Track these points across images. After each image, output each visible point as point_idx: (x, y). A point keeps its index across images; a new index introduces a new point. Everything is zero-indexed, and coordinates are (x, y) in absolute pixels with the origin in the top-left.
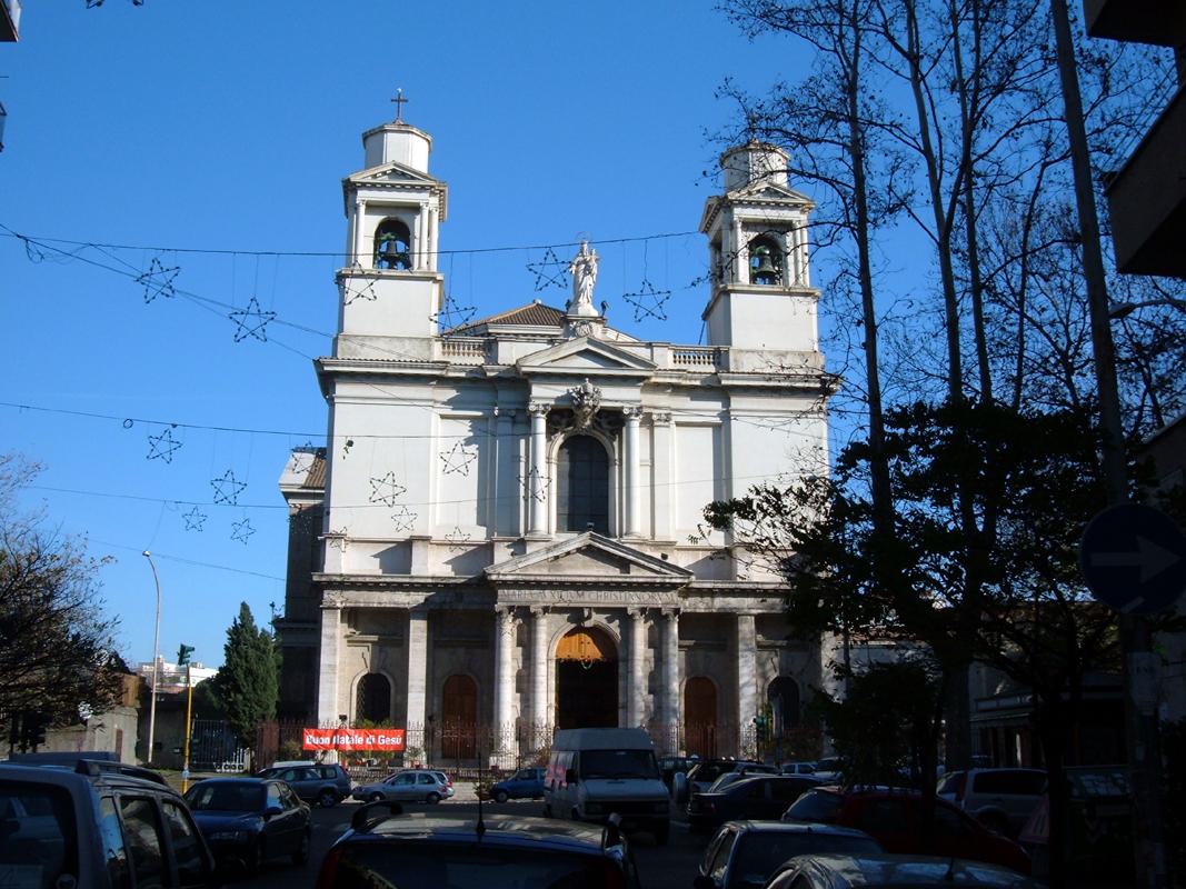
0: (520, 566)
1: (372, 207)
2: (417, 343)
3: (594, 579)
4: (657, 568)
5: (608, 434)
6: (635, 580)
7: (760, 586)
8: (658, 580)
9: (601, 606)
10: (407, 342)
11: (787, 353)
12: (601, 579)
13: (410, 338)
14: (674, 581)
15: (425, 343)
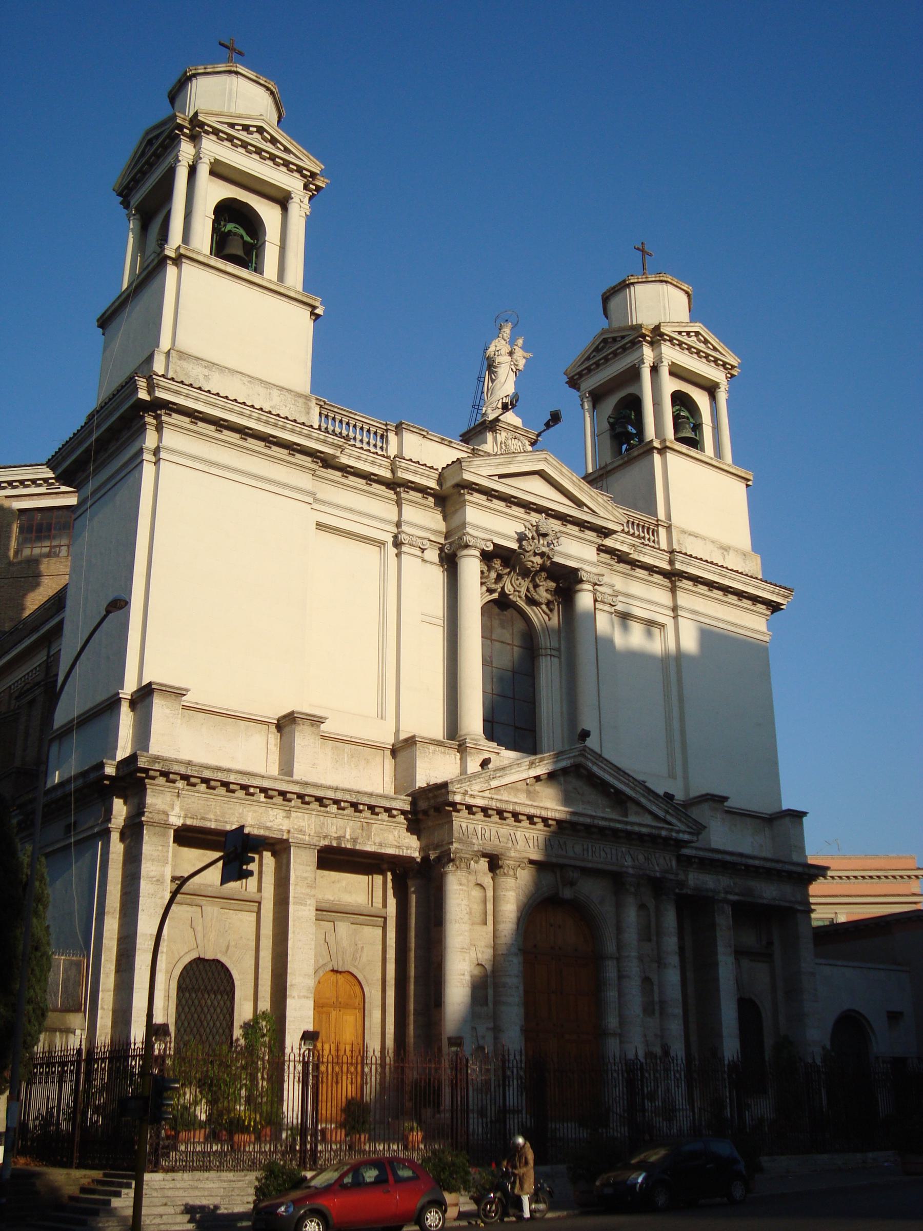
0: (494, 784)
1: (219, 171)
2: (289, 396)
3: (588, 820)
4: (661, 814)
5: (544, 607)
6: (636, 829)
7: (744, 860)
8: (664, 833)
9: (590, 865)
10: (275, 392)
11: (729, 548)
12: (596, 822)
13: (282, 388)
14: (681, 836)
15: (301, 400)
